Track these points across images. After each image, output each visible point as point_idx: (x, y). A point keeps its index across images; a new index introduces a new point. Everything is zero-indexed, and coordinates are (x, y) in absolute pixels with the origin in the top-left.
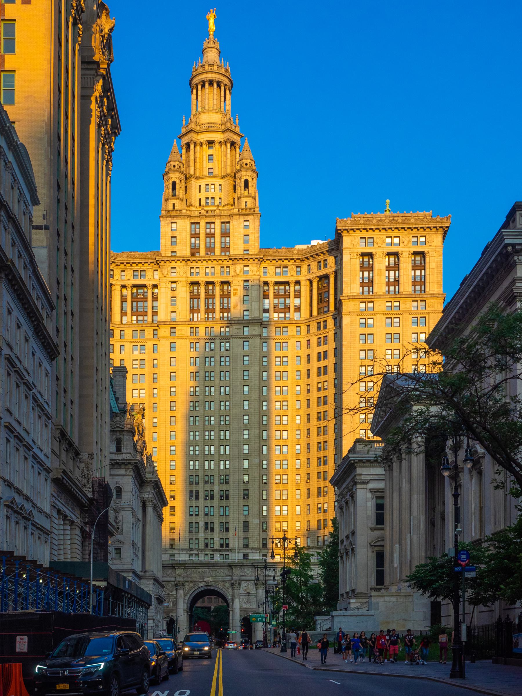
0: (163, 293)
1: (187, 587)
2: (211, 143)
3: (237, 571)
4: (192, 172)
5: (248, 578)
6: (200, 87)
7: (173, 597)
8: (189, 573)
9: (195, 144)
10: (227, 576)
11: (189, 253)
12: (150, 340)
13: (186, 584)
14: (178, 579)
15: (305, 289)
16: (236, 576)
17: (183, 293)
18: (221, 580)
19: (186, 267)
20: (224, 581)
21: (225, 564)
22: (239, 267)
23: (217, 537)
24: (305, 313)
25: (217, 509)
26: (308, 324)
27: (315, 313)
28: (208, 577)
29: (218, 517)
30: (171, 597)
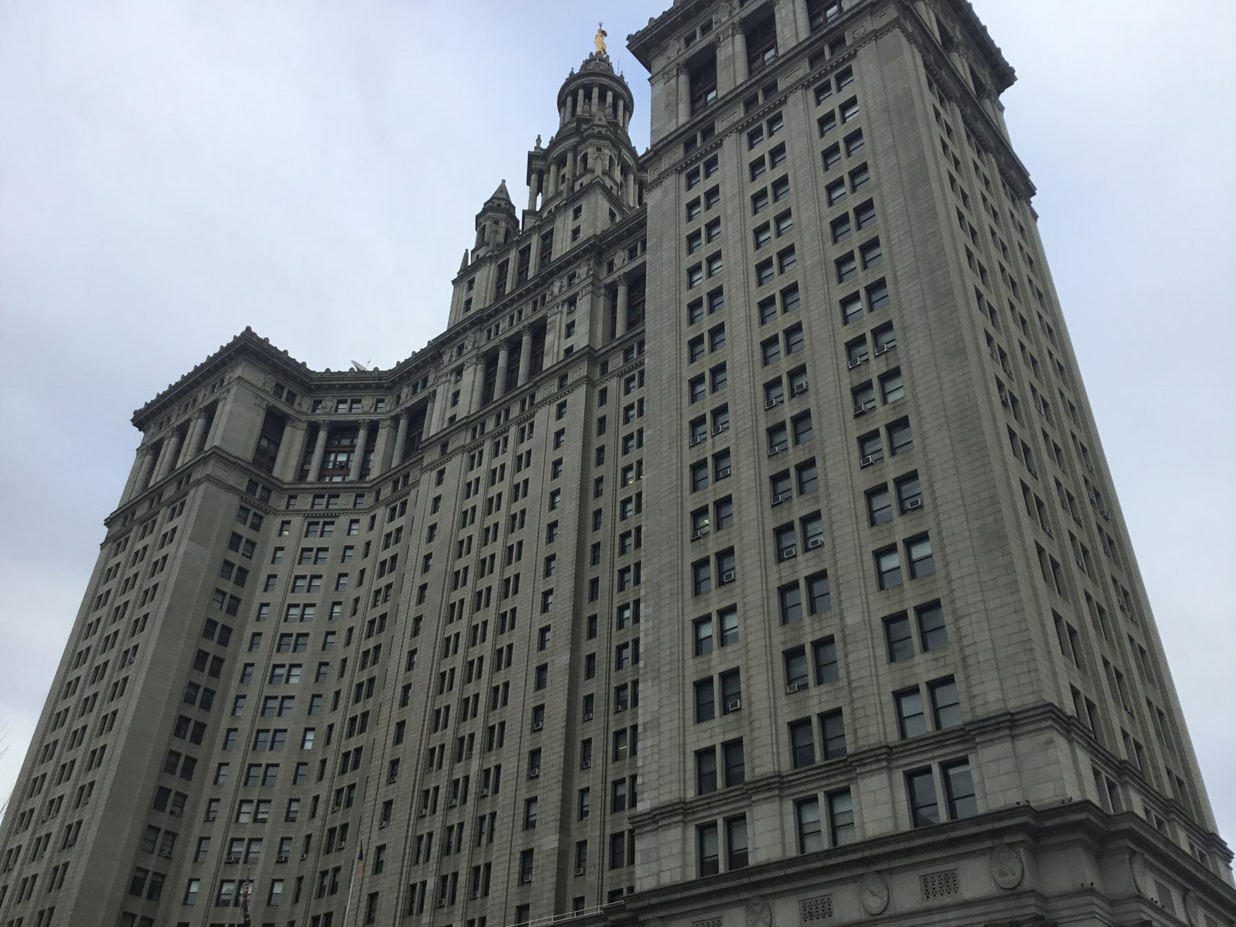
17: (472, 378)
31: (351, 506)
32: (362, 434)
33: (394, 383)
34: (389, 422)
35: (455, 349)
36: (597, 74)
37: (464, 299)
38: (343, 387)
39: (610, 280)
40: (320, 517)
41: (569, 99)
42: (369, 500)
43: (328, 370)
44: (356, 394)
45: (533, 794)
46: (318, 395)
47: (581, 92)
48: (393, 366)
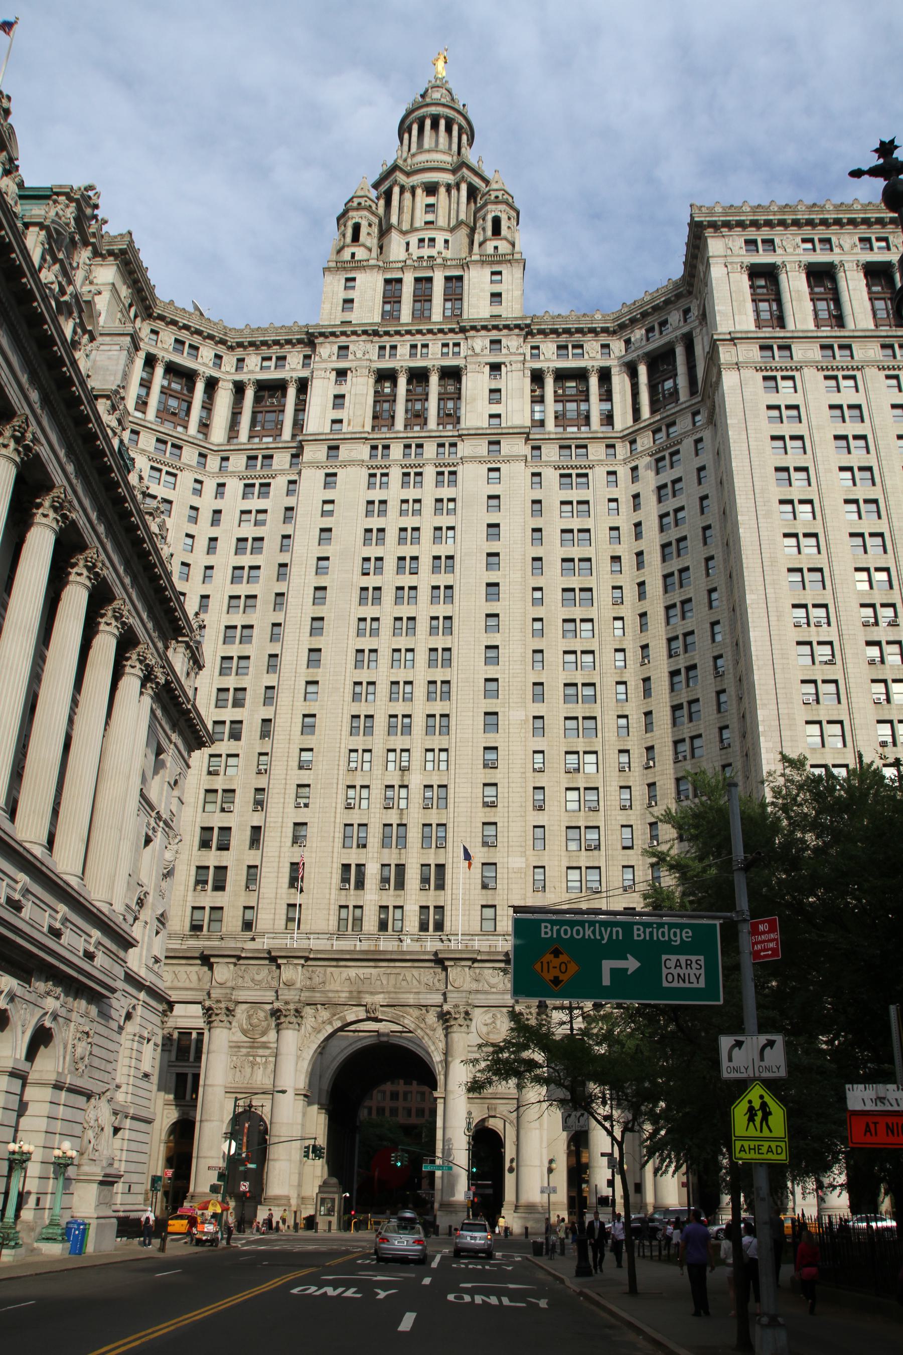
0: (322, 391)
1: (309, 1021)
2: (431, 189)
3: (459, 975)
4: (394, 220)
5: (493, 999)
6: (415, 127)
7: (267, 1052)
8: (316, 980)
9: (402, 189)
10: (430, 989)
11: (377, 319)
12: (282, 472)
13: (308, 1011)
14: (286, 995)
15: (620, 383)
16: (457, 989)
17: (361, 390)
18: (412, 1002)
19: (369, 346)
20: (420, 1007)
21: (425, 953)
22: (480, 342)
23: (413, 898)
24: (623, 419)
25: (415, 830)
26: (631, 437)
27: (646, 412)
28: (372, 993)
29: (415, 850)
30: (261, 1052)
31: (194, 463)
32: (200, 386)
33: (240, 345)
34: (231, 386)
35: (335, 348)
36: (444, 105)
37: (342, 295)
38: (186, 327)
39: (537, 365)
40: (164, 464)
41: (428, 123)
42: (213, 462)
43: (172, 302)
44: (196, 340)
45: (492, 820)
46: (159, 325)
47: (442, 123)
48: (240, 325)
